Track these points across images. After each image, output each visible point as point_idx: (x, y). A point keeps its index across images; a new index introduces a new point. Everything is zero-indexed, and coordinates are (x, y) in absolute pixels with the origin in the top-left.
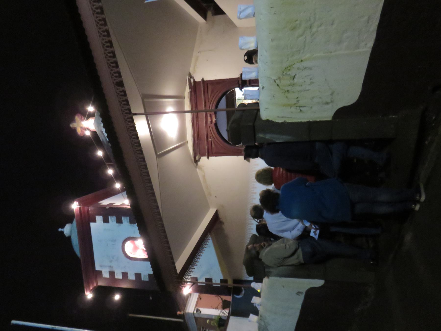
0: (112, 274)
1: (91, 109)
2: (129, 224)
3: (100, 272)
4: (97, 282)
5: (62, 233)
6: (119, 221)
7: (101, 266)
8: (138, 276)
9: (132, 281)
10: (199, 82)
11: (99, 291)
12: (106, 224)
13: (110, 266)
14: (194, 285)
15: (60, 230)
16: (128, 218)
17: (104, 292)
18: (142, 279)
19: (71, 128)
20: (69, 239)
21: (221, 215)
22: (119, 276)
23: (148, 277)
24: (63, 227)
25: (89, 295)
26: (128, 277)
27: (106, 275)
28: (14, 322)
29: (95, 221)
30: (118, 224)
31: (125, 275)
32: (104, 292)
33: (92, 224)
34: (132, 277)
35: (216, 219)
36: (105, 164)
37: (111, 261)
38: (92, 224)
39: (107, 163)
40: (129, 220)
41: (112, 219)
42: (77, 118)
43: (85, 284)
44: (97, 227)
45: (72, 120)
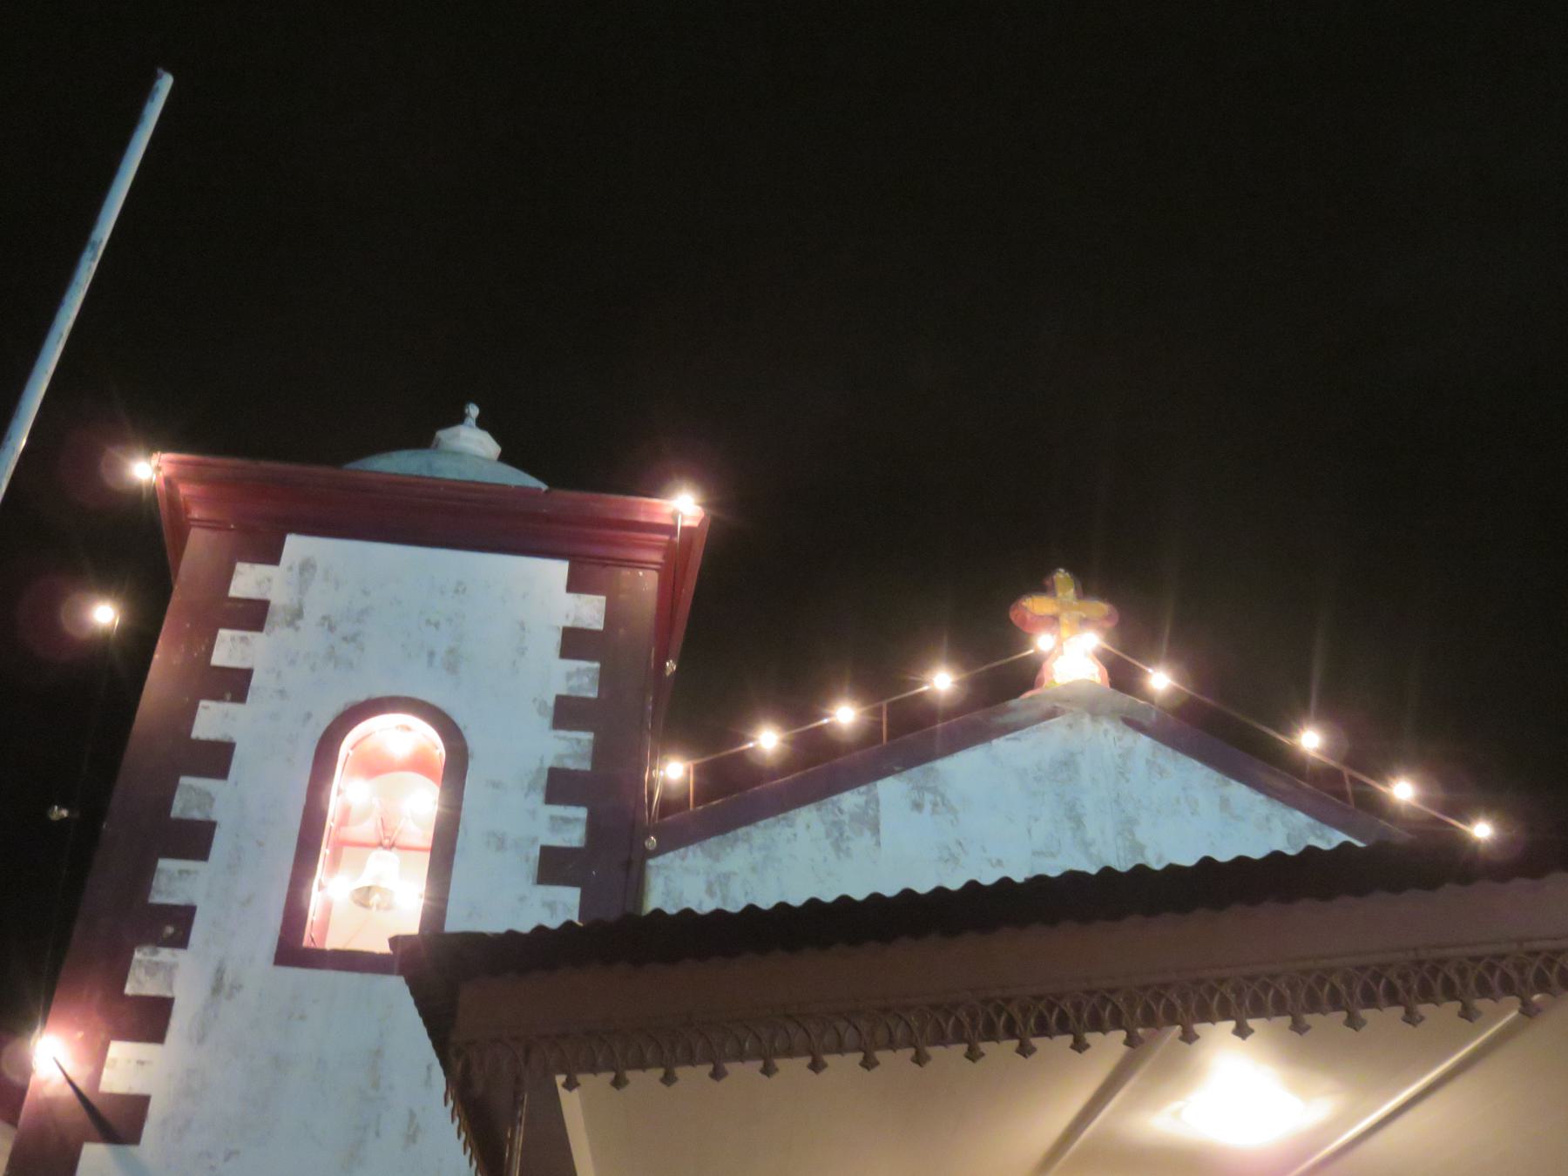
0: (253, 615)
1: (1160, 680)
2: (549, 762)
3: (271, 555)
4: (202, 524)
5: (460, 419)
7: (307, 567)
8: (216, 759)
12: (558, 637)
13: (298, 614)
14: (81, 1115)
15: (473, 411)
16: (586, 766)
17: (137, 548)
18: (185, 781)
19: (1052, 569)
20: (422, 439)
22: (228, 649)
23: (197, 815)
25: (146, 470)
26: (218, 697)
27: (247, 581)
28: (165, 83)
29: (576, 584)
30: (551, 702)
31: (235, 685)
33: (558, 570)
34: (211, 720)
36: (882, 698)
37: (329, 624)
38: (558, 570)
39: (884, 704)
40: (571, 765)
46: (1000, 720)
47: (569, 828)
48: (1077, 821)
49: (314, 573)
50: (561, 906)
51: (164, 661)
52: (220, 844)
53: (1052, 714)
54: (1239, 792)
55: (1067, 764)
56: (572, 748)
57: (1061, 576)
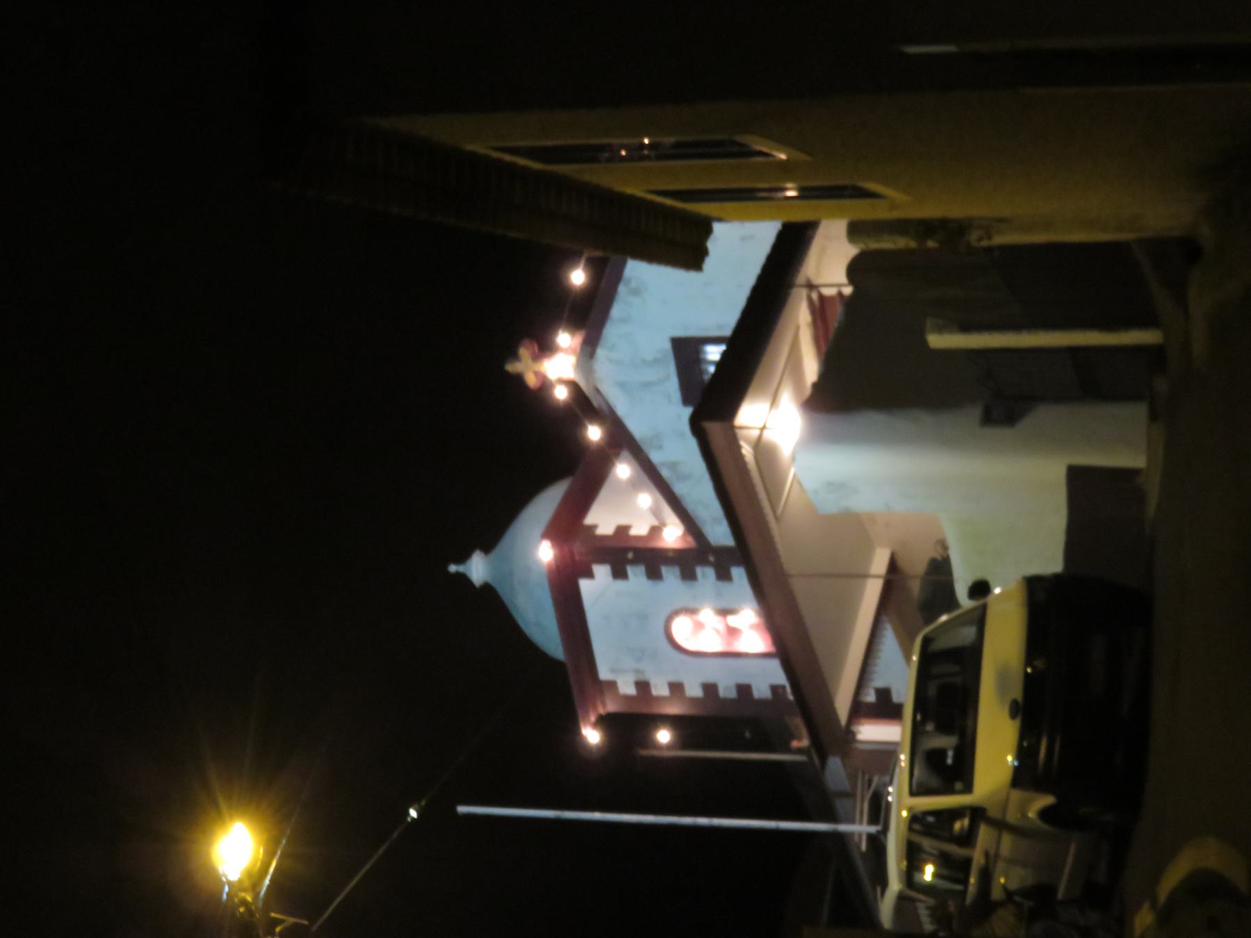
0: (643, 686)
3: (612, 685)
4: (604, 705)
5: (463, 579)
6: (654, 574)
7: (613, 671)
8: (710, 689)
9: (694, 701)
10: (831, 298)
11: (606, 722)
13: (637, 671)
15: (453, 568)
19: (508, 375)
21: (902, 563)
24: (463, 557)
25: (592, 736)
27: (627, 687)
28: (462, 809)
29: (589, 575)
31: (676, 688)
32: (629, 726)
34: (694, 690)
35: (893, 567)
38: (584, 584)
41: (636, 574)
42: (524, 352)
43: (580, 712)
44: (597, 588)
45: (514, 356)
46: (604, 407)
47: (706, 574)
48: (647, 385)
49: (617, 666)
50: (738, 573)
51: (674, 709)
52: (743, 680)
53: (597, 390)
54: (616, 311)
55: (622, 385)
56: (671, 575)
57: (511, 367)
